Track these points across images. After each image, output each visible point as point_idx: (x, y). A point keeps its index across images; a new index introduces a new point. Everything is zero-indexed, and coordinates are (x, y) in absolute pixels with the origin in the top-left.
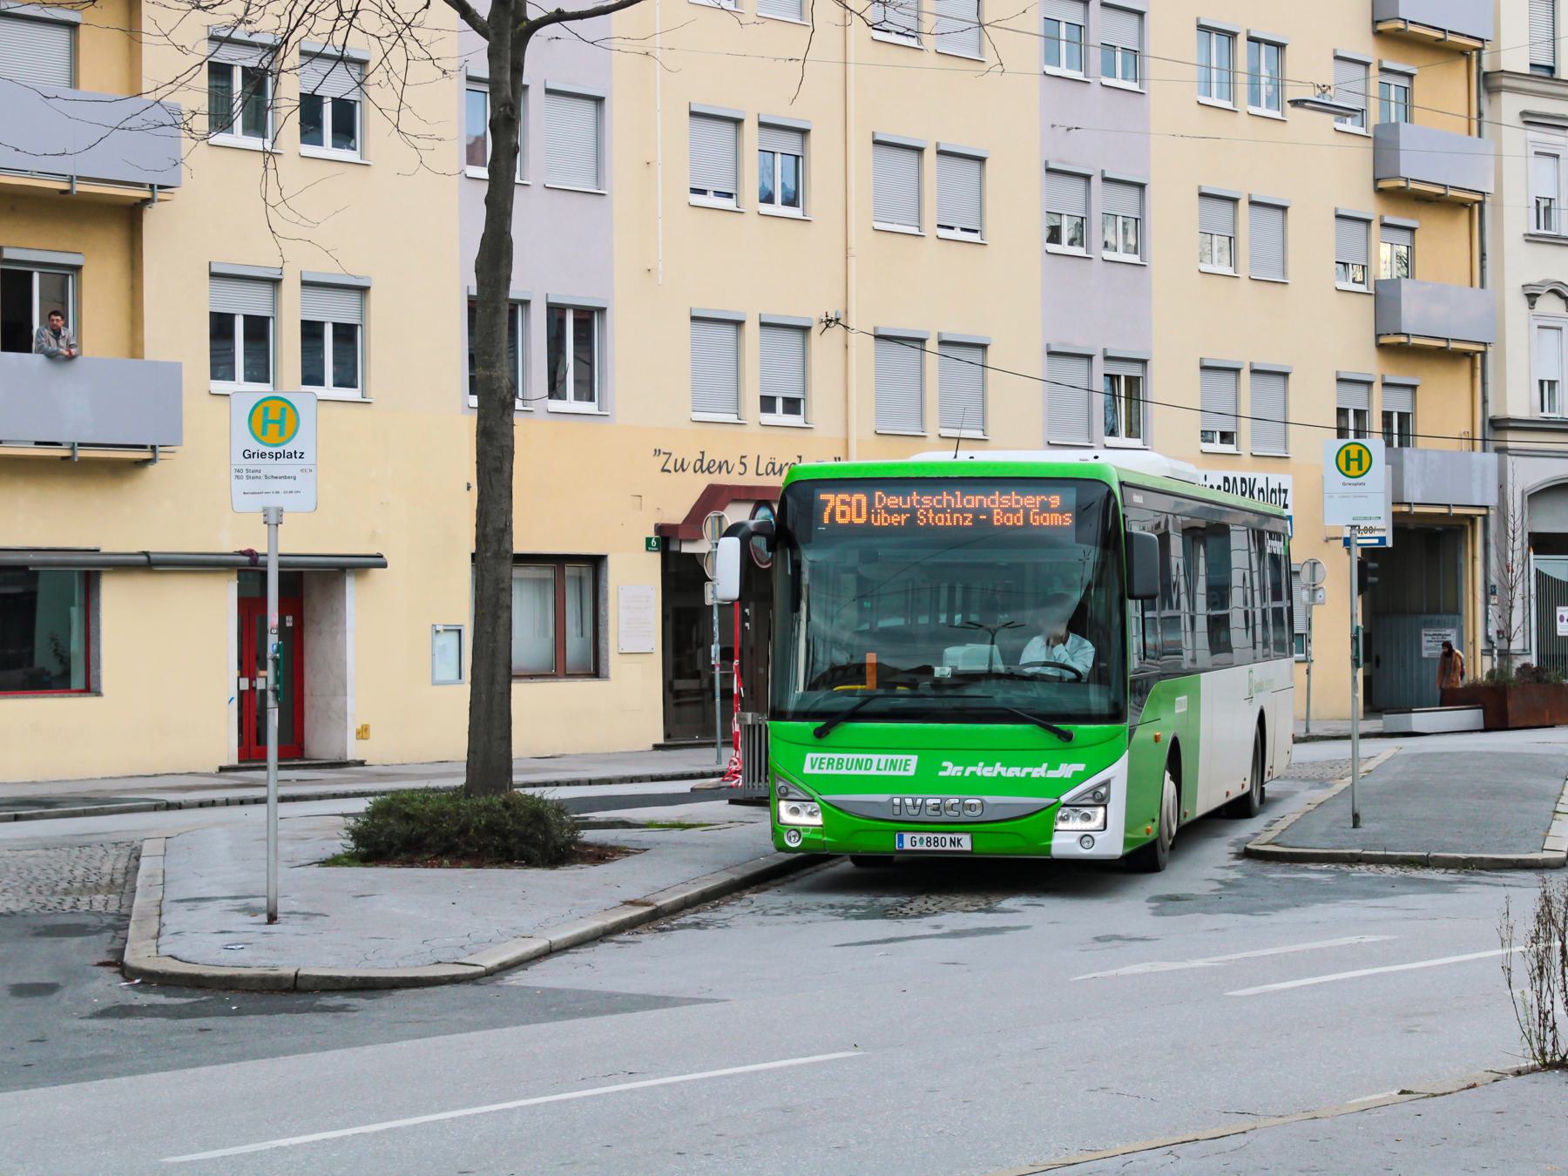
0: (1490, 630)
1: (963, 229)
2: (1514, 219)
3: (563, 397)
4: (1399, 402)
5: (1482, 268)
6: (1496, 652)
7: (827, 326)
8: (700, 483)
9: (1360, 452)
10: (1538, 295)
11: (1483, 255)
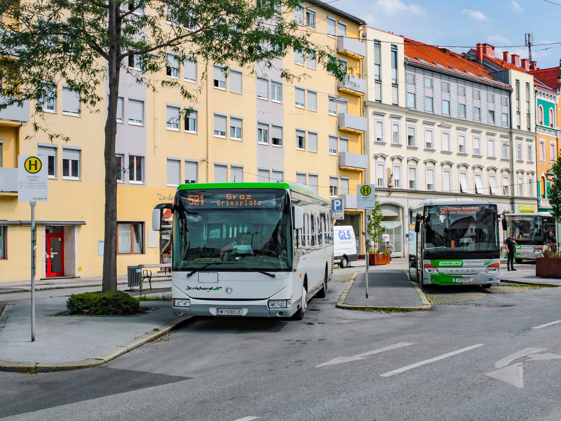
2: (372, 139)
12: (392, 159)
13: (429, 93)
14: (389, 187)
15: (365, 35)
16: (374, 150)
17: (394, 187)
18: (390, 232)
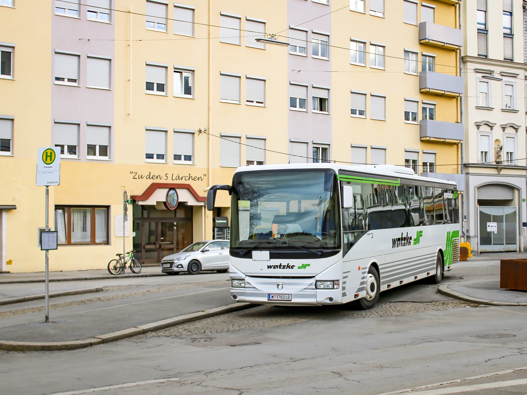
0: (463, 229)
1: (257, 102)
4: (429, 159)
5: (461, 117)
6: (465, 236)
7: (200, 132)
8: (150, 182)
9: (51, 153)
10: (480, 125)
11: (461, 113)
12: (503, 128)
14: (498, 162)
17: (506, 163)
18: (497, 219)
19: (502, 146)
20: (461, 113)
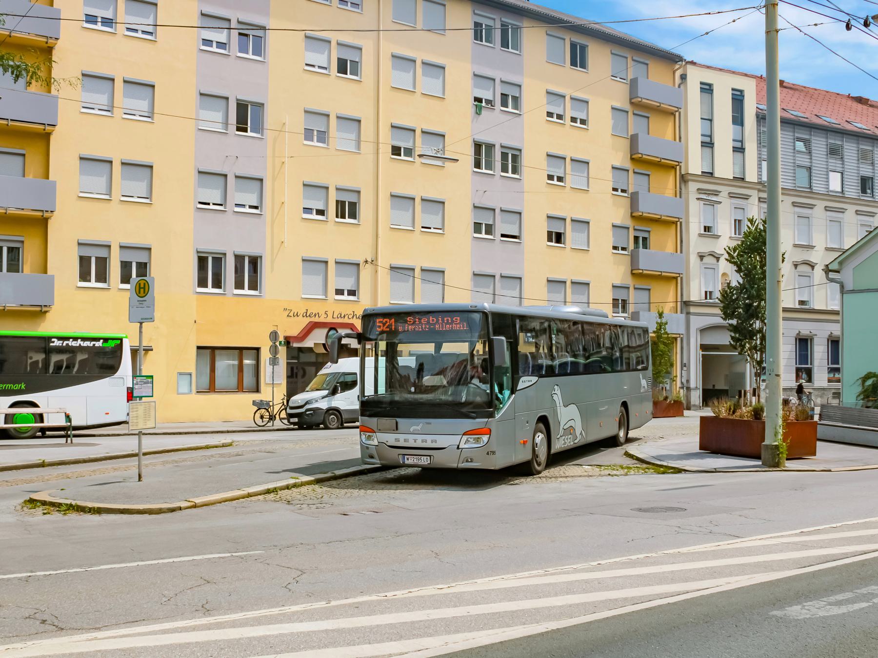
2: (695, 228)
3: (243, 288)
6: (685, 388)
8: (307, 320)
11: (681, 241)
13: (804, 160)
15: (684, 76)
16: (695, 243)
19: (730, 281)
20: (681, 241)
